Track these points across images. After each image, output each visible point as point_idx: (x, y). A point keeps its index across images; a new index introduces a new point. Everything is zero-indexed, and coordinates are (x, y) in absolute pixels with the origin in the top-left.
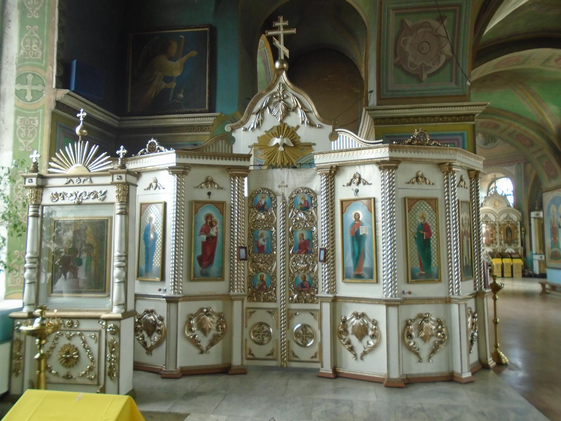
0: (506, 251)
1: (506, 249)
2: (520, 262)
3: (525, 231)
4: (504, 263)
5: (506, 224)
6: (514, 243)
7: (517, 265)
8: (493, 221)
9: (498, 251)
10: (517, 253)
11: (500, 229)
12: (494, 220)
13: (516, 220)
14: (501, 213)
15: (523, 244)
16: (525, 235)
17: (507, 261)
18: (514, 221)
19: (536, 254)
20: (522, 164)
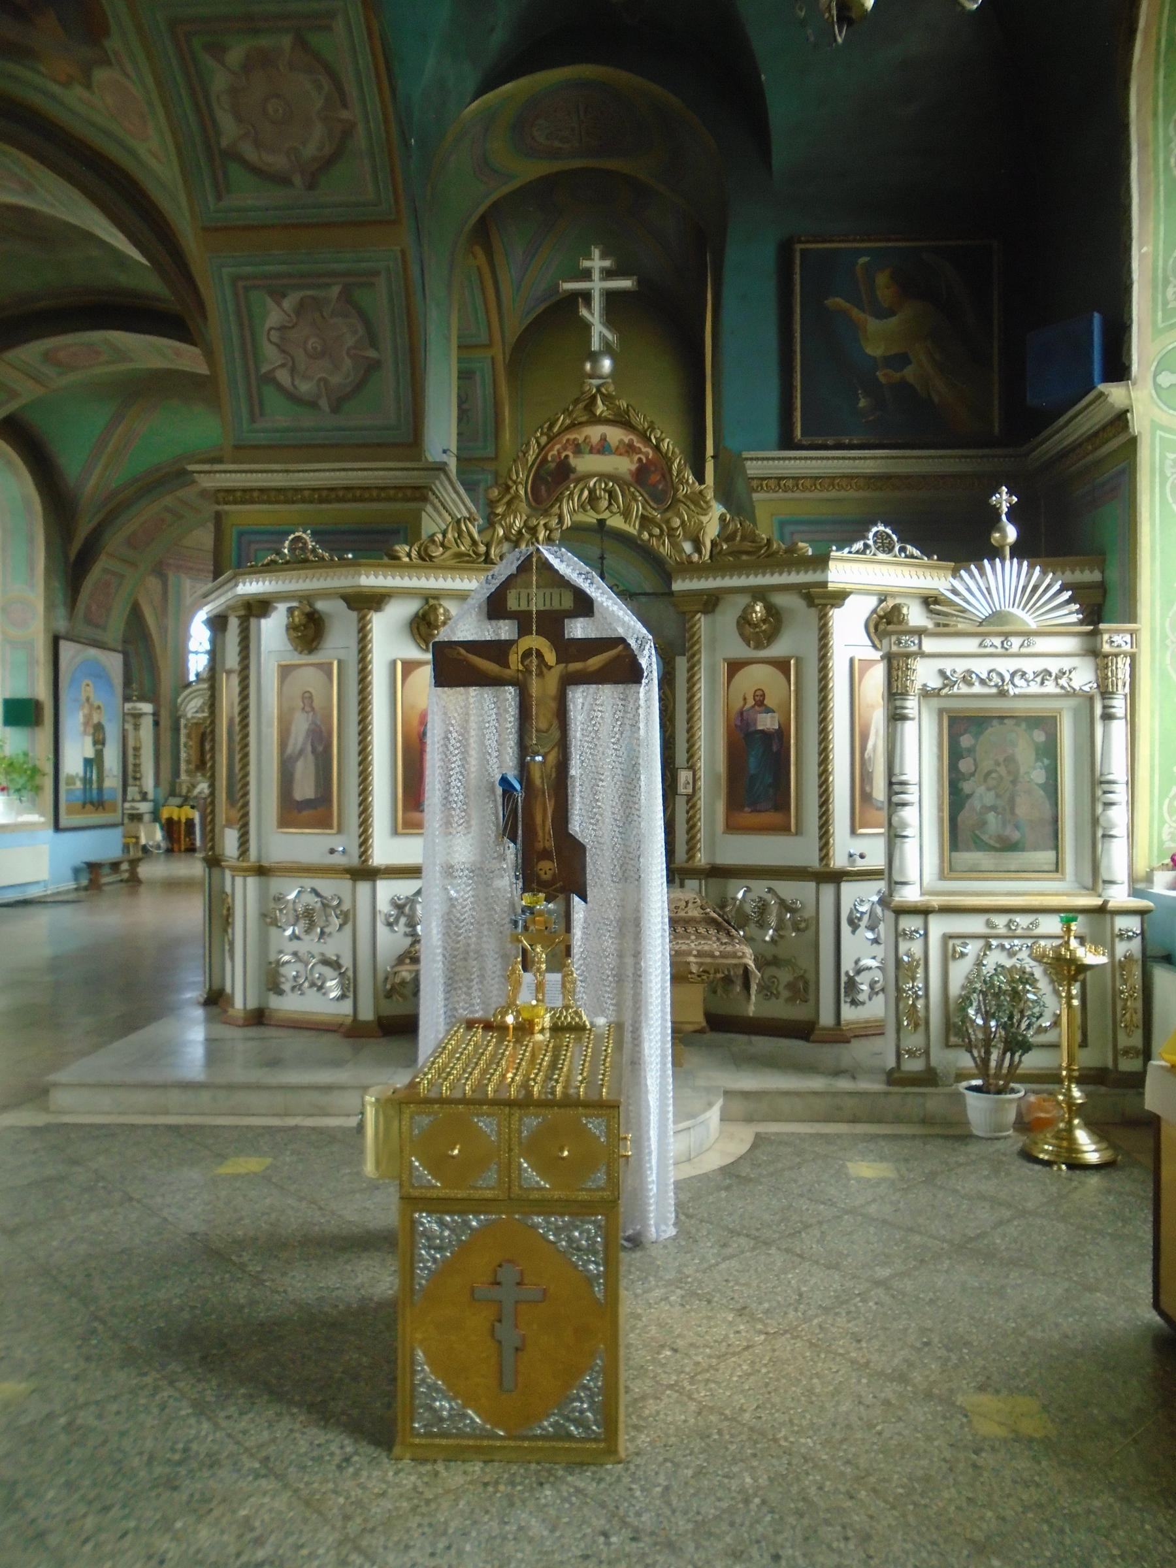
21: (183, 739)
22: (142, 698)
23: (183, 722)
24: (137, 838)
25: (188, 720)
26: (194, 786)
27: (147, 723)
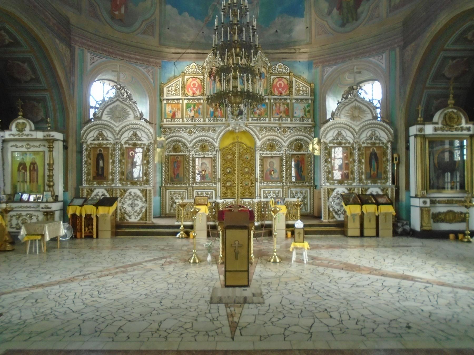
0: (368, 193)
1: (368, 189)
2: (390, 209)
3: (399, 159)
4: (365, 212)
5: (370, 147)
6: (381, 179)
7: (386, 214)
8: (349, 143)
9: (356, 191)
10: (386, 194)
11: (360, 155)
12: (352, 142)
13: (385, 141)
14: (363, 129)
15: (395, 181)
16: (398, 164)
17: (370, 209)
18: (383, 143)
19: (416, 197)
20: (398, 50)
21: (84, 159)
22: (56, 130)
23: (84, 146)
24: (43, 236)
25: (88, 145)
26: (92, 191)
27: (59, 147)
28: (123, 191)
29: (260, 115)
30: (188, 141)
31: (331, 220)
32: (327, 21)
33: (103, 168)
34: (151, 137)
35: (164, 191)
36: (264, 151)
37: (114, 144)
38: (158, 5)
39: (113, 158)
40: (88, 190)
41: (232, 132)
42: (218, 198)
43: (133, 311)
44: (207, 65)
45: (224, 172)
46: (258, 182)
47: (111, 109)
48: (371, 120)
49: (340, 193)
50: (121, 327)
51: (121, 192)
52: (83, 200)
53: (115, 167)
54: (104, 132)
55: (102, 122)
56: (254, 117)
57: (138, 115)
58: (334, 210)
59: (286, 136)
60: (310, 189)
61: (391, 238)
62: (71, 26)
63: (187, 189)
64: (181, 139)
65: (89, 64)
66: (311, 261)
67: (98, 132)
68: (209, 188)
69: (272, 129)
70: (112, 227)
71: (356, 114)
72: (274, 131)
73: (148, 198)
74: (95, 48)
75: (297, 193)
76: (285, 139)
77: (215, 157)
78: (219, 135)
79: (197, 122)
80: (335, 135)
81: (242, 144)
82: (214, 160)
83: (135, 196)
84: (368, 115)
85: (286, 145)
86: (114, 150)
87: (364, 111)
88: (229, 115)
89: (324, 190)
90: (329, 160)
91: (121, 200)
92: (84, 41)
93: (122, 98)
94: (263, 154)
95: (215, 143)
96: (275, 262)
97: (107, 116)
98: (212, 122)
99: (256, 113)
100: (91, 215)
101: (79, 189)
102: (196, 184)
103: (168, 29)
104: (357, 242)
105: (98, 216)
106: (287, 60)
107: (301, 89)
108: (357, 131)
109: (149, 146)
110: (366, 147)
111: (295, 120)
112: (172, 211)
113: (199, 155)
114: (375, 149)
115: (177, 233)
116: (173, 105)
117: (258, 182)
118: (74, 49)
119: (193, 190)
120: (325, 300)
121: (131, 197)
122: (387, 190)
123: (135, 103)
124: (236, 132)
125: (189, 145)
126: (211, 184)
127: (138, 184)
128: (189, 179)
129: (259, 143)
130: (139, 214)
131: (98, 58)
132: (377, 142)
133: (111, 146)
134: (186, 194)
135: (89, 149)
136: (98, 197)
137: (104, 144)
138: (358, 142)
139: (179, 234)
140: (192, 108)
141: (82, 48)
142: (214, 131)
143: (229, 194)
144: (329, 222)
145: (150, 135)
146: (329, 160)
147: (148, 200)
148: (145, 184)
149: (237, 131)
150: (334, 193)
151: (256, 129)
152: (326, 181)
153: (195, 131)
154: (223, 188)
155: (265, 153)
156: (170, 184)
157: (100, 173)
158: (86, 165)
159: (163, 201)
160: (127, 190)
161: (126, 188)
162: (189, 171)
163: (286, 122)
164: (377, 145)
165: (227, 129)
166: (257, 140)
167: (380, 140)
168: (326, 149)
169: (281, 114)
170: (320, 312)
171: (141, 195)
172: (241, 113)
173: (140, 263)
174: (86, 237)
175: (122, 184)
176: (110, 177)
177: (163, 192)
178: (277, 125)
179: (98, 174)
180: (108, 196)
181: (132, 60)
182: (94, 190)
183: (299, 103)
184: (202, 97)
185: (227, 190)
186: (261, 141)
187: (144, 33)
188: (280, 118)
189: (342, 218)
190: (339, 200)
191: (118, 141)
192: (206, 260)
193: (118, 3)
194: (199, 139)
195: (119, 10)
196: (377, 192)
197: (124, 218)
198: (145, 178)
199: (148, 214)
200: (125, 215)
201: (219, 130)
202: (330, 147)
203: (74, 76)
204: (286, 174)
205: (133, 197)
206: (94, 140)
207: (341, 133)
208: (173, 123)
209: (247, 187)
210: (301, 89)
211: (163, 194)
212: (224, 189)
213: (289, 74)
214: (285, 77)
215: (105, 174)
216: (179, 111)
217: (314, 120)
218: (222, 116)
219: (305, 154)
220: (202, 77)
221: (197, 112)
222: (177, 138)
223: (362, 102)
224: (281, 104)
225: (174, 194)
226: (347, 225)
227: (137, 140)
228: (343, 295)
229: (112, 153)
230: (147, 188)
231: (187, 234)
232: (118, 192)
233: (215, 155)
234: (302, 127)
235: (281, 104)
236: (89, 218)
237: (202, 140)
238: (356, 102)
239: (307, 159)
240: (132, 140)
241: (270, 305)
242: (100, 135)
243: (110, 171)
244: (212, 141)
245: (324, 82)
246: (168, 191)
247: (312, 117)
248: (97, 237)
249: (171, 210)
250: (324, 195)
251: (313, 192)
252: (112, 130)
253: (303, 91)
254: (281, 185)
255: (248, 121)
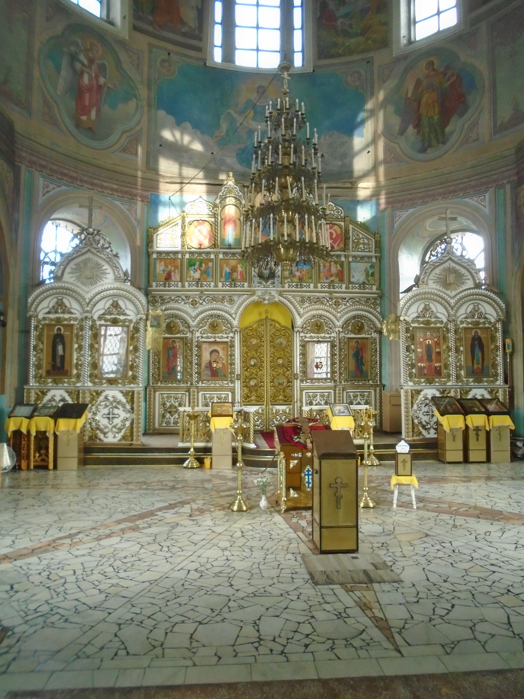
0: (469, 397)
1: (470, 390)
2: (506, 421)
4: (470, 426)
6: (488, 376)
7: (500, 429)
8: (442, 322)
9: (452, 394)
10: (497, 398)
11: (458, 340)
12: (445, 320)
13: (493, 320)
14: (461, 302)
16: (512, 354)
18: (490, 323)
20: (508, 187)
21: (33, 342)
23: (33, 323)
25: (39, 321)
26: (44, 393)
28: (94, 394)
29: (301, 279)
30: (191, 317)
31: (415, 438)
32: (398, 144)
33: (63, 357)
34: (141, 309)
35: (152, 393)
36: (307, 333)
37: (82, 320)
38: (146, 109)
39: (79, 342)
40: (37, 391)
41: (257, 304)
42: (237, 404)
43: (193, 602)
44: (220, 202)
45: (245, 366)
46: (299, 380)
47: (77, 265)
48: (472, 288)
49: (430, 397)
50: (192, 635)
51: (92, 395)
52: (31, 409)
53: (83, 356)
54: (65, 301)
55: (63, 285)
56: (292, 282)
57: (122, 275)
58: (420, 423)
59: (339, 310)
60: (375, 391)
61: (510, 465)
62: (16, 135)
63: (188, 391)
64: (179, 313)
65: (41, 194)
66: (421, 505)
67: (55, 300)
68: (222, 389)
69: (318, 301)
70: (80, 451)
71: (451, 278)
72: (323, 303)
73: (135, 406)
74: (51, 170)
75: (355, 397)
76: (339, 315)
77: (231, 341)
78: (239, 307)
79: (205, 288)
80: (420, 309)
81: (273, 323)
82: (232, 346)
83: (115, 401)
84: (467, 281)
85: (339, 324)
86: (82, 328)
87: (463, 275)
88: (254, 279)
89: (406, 392)
90: (413, 347)
91: (91, 408)
92: (34, 159)
93: (95, 249)
94: (306, 337)
95: (232, 320)
96: (366, 507)
97: (71, 275)
98: (227, 288)
99: (294, 276)
100: (45, 432)
101: (24, 389)
102: (202, 383)
103: (161, 146)
104: (458, 471)
105: (57, 433)
106: (341, 199)
107: (361, 241)
108: (453, 304)
109: (137, 323)
110: (465, 329)
111: (353, 288)
112: (164, 424)
113: (207, 337)
114: (478, 331)
115: (186, 459)
116: (168, 261)
117: (299, 380)
118: (20, 167)
119: (198, 392)
120: (494, 572)
121: (108, 403)
122: (497, 392)
123: (116, 256)
124: (265, 304)
125: (192, 323)
126: (225, 382)
127: (119, 383)
128: (191, 376)
129: (299, 322)
130: (120, 430)
131: (55, 186)
132: (482, 321)
133: (76, 323)
134: (187, 398)
135: (41, 326)
136: (54, 404)
137: (66, 320)
138: (454, 321)
139: (187, 462)
140: (196, 267)
141: (30, 169)
142: (231, 301)
143: (253, 398)
144: (414, 440)
145: (140, 306)
146: (413, 347)
147: (135, 408)
148: (130, 383)
149: (266, 302)
150: (421, 397)
151: (296, 300)
152: (408, 378)
153: (201, 302)
154: (245, 388)
155: (308, 335)
156: (161, 382)
157: (58, 364)
158: (35, 353)
159: (150, 408)
160: (101, 392)
161: (99, 389)
162: (191, 363)
163: (340, 290)
164: (481, 326)
165: (252, 299)
166: (297, 317)
167: (485, 318)
168: (407, 330)
169: (333, 278)
170: (503, 594)
171: (124, 400)
172: (272, 275)
173: (151, 514)
174: (36, 467)
175: (94, 383)
176: (75, 372)
177: (150, 394)
178: (327, 294)
179: (54, 367)
180: (70, 401)
181: (105, 191)
182: (46, 392)
183: (359, 262)
184: (212, 250)
185: (250, 391)
186: (303, 318)
187: (124, 150)
188: (331, 284)
189: (432, 434)
190: (427, 407)
191: (89, 315)
192: (258, 506)
193: (87, 103)
194: (207, 313)
195: (87, 113)
196: (483, 395)
197: (96, 437)
198: (130, 373)
199: (135, 430)
200: (98, 432)
201: (238, 301)
202: (413, 328)
203: (19, 212)
204: (340, 369)
205: (111, 403)
206: (49, 313)
207: (430, 308)
208: (167, 288)
209: (280, 387)
210: (361, 241)
211: (150, 398)
212: (246, 390)
213: (344, 219)
214: (338, 223)
215: (66, 367)
216: (177, 271)
217: (380, 288)
218: (243, 280)
219: (367, 338)
220: (213, 220)
221: (205, 273)
222: (174, 311)
223: (459, 262)
224: (332, 263)
225: (167, 397)
226: (444, 445)
227: (119, 314)
228: (516, 563)
229: (78, 333)
230: (135, 389)
231: (201, 461)
232: (88, 395)
233: (232, 338)
234: (363, 297)
235: (332, 263)
236: (42, 436)
237: (212, 316)
238: (450, 262)
239: (369, 345)
240: (111, 314)
241: (414, 585)
242: (60, 305)
243: (75, 361)
244: (228, 316)
245: (394, 232)
246: (157, 393)
247: (377, 283)
248: (55, 467)
249: (162, 422)
250: (406, 400)
251: (381, 394)
252: (78, 297)
253: (364, 244)
254: (332, 384)
255: (283, 287)
